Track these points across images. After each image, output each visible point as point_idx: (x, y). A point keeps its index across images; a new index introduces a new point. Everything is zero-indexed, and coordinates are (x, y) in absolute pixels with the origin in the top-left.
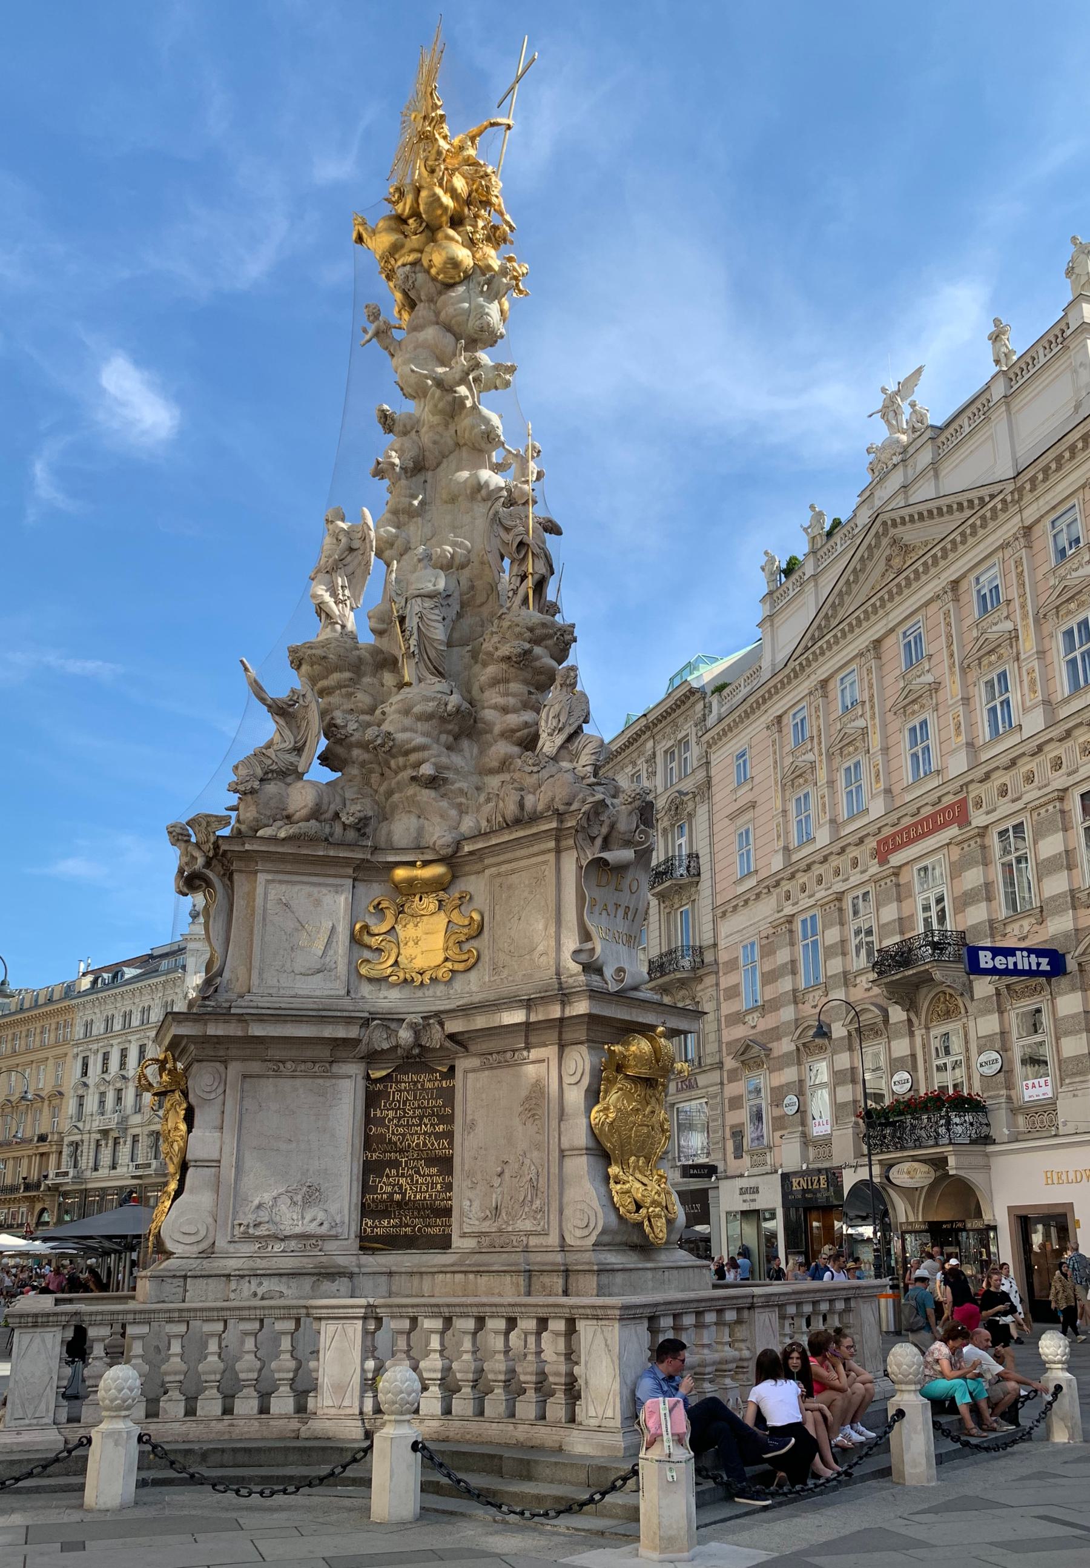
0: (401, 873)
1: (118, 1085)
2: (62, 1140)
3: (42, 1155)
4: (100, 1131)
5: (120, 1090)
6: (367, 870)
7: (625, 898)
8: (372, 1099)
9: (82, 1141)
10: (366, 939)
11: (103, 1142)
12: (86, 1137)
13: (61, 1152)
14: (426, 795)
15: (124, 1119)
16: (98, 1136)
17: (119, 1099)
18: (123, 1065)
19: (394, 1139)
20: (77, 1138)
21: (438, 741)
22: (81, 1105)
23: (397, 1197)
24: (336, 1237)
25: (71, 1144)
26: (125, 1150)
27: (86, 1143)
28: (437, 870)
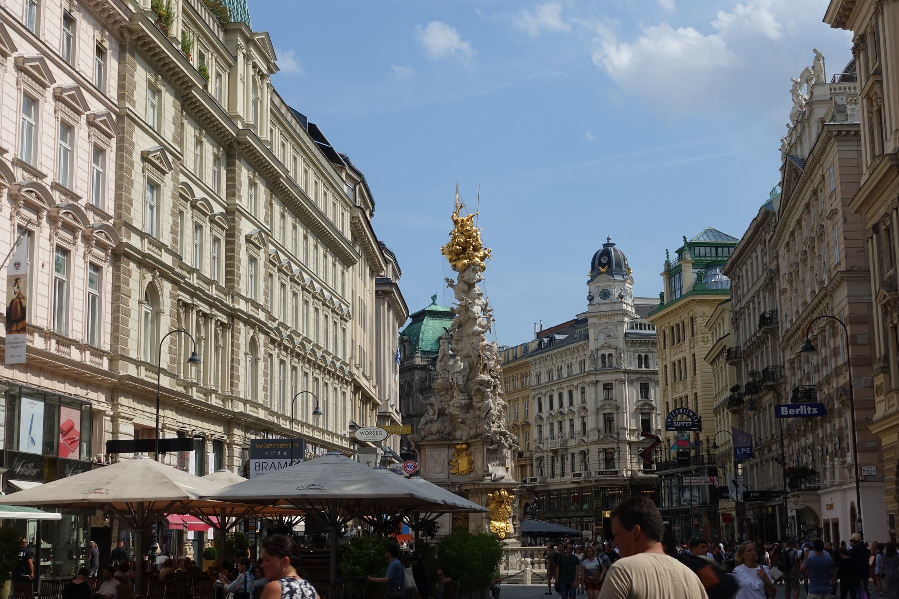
0: (458, 447)
1: (559, 419)
2: (532, 456)
4: (552, 451)
5: (561, 423)
6: (449, 446)
7: (499, 456)
12: (545, 454)
13: (532, 465)
14: (462, 426)
15: (565, 442)
17: (561, 428)
18: (561, 406)
20: (540, 455)
22: (541, 432)
25: (538, 458)
26: (568, 463)
28: (464, 446)
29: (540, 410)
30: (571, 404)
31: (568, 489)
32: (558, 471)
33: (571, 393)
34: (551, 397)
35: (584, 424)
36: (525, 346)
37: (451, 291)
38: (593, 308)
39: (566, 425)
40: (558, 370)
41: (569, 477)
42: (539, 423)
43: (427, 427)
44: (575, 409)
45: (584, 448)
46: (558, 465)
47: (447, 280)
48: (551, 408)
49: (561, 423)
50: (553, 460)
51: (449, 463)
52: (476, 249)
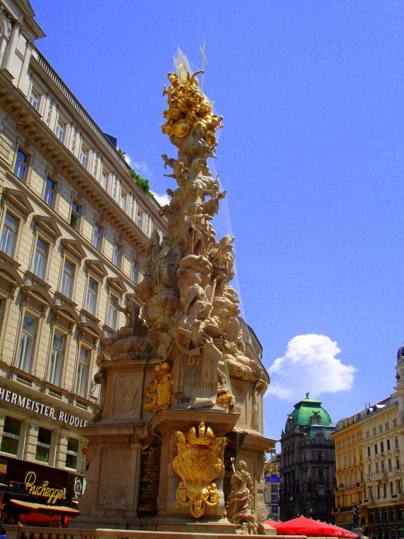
1: (382, 459)
2: (365, 485)
3: (360, 493)
4: (378, 481)
5: (383, 462)
8: (144, 458)
9: (372, 486)
10: (148, 395)
11: (380, 486)
15: (386, 475)
16: (377, 483)
17: (383, 466)
18: (382, 450)
19: (149, 473)
20: (370, 484)
21: (164, 315)
23: (148, 496)
24: (128, 510)
26: (388, 489)
27: (374, 487)
29: (369, 455)
30: (389, 448)
31: (389, 507)
32: (382, 494)
33: (388, 441)
34: (376, 446)
35: (398, 462)
36: (359, 415)
37: (170, 171)
38: (400, 383)
39: (386, 463)
40: (380, 427)
41: (389, 498)
42: (369, 463)
43: (119, 342)
44: (391, 452)
45: (398, 478)
46: (382, 490)
47: (165, 157)
48: (376, 453)
49: (383, 462)
50: (379, 488)
51: (143, 395)
52: (202, 114)
